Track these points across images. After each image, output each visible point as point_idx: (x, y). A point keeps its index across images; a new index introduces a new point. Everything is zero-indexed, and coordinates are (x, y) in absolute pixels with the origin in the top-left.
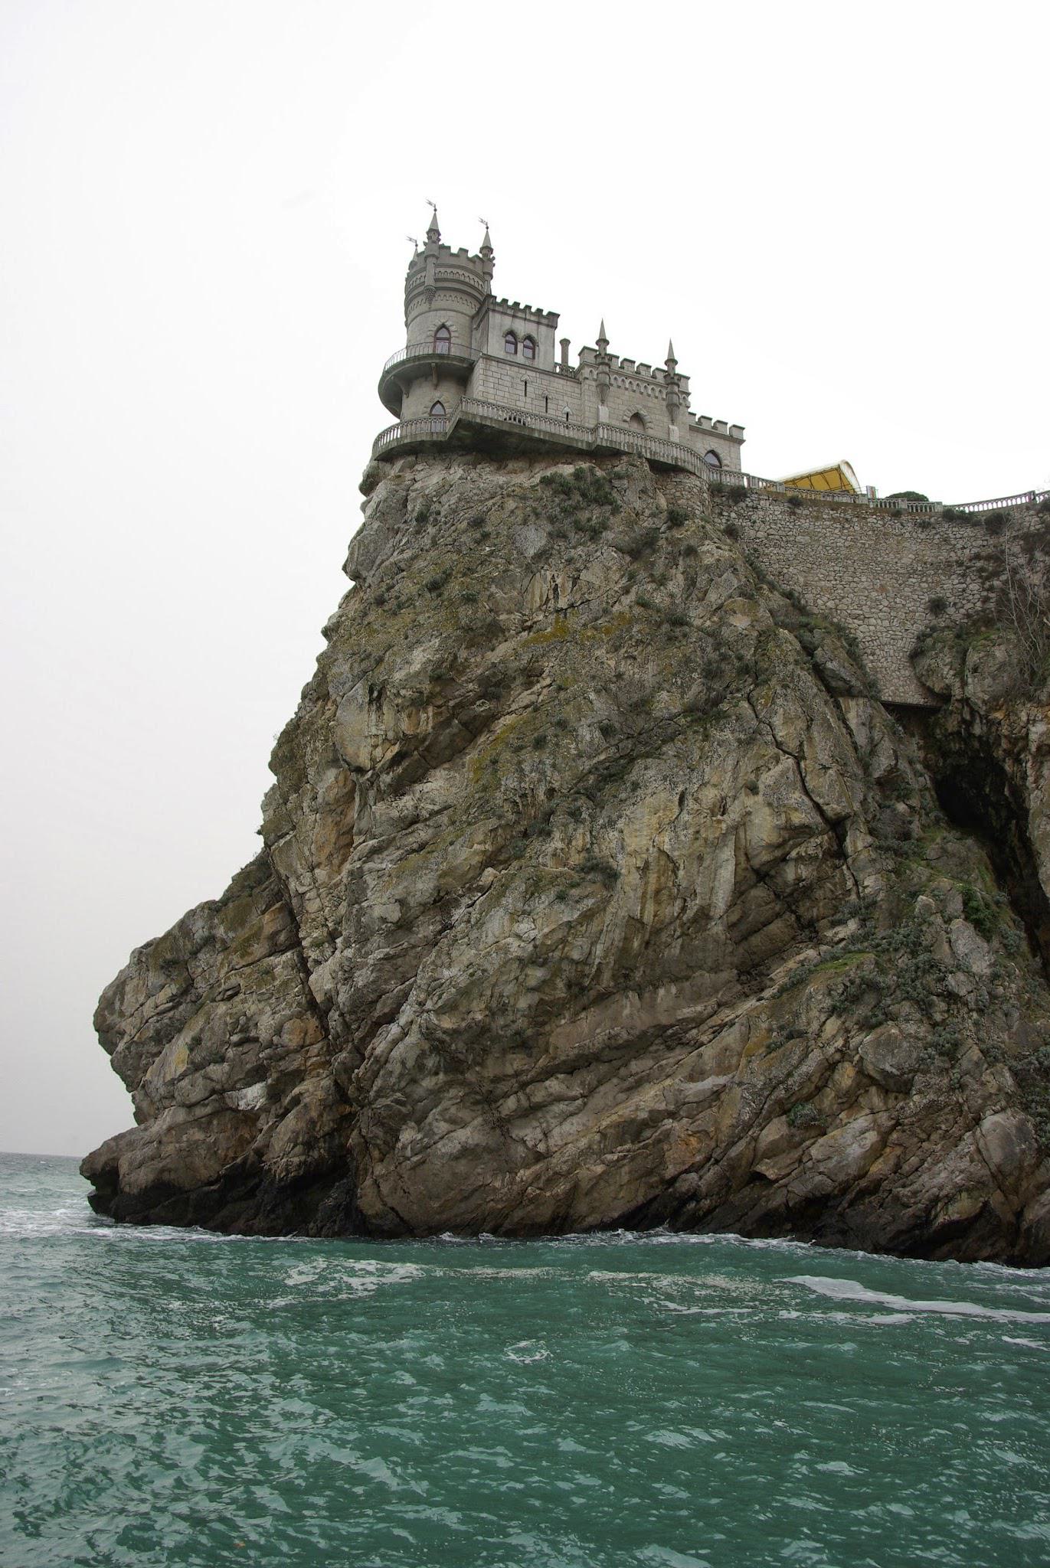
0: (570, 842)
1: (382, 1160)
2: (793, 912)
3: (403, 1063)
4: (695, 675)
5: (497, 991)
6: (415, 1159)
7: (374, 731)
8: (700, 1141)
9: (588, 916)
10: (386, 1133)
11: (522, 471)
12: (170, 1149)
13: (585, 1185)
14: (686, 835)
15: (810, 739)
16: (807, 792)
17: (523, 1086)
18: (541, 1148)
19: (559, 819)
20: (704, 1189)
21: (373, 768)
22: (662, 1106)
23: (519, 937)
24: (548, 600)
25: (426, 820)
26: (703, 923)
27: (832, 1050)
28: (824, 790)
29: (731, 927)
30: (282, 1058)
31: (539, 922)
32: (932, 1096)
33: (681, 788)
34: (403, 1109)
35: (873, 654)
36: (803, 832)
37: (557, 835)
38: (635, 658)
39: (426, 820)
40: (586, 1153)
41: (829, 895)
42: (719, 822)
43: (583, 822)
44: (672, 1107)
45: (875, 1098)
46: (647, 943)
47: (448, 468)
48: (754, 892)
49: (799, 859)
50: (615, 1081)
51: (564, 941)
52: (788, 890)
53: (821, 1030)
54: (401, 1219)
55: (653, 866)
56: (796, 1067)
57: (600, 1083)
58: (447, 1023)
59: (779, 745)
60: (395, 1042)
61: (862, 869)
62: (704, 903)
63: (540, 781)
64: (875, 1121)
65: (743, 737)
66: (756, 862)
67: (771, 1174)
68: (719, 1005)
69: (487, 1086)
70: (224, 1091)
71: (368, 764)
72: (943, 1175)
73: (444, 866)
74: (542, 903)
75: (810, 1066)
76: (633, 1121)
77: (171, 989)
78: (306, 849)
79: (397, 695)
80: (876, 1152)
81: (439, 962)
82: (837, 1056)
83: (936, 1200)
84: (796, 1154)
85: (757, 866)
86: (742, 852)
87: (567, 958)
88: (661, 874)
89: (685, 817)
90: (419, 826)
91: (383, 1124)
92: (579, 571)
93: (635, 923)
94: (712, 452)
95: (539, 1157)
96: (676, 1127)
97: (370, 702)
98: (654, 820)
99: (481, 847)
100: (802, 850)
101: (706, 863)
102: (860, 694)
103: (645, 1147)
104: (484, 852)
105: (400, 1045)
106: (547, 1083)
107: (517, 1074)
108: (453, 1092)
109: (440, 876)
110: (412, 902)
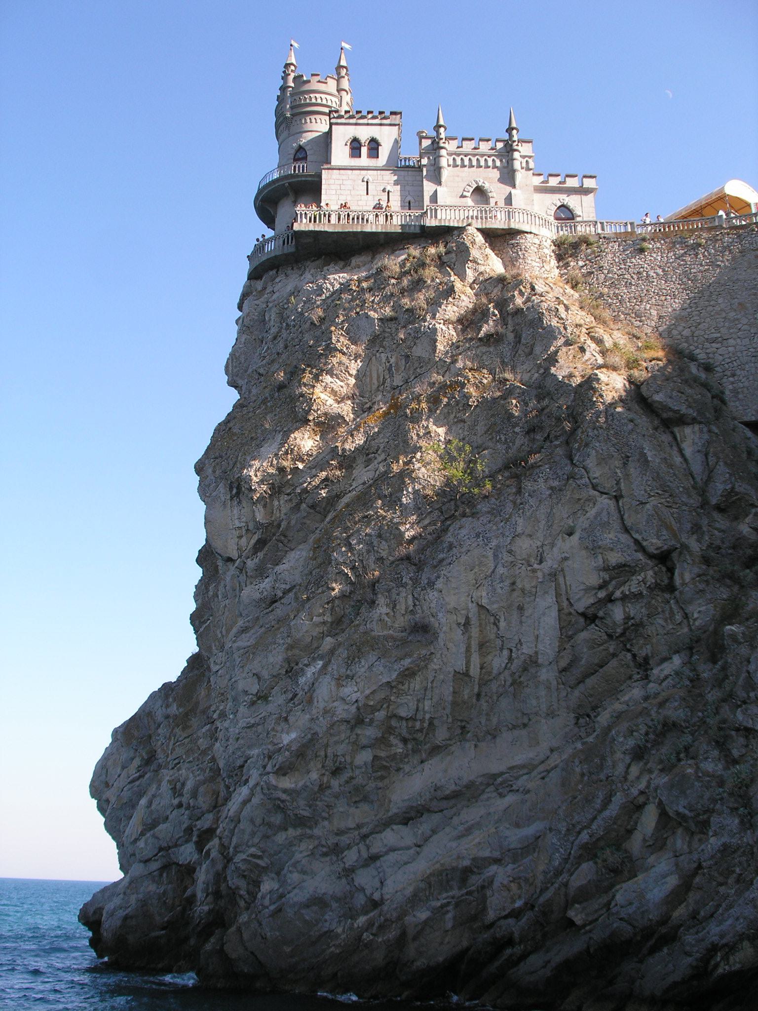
0: (394, 606)
1: (247, 909)
2: (629, 651)
3: (252, 821)
4: (517, 429)
5: (330, 751)
6: (272, 908)
7: (237, 524)
8: (520, 887)
9: (408, 674)
10: (248, 884)
11: (364, 265)
12: (133, 899)
13: (411, 932)
15: (627, 476)
16: (627, 530)
17: (364, 837)
18: (377, 896)
20: (516, 935)
21: (240, 557)
22: (486, 853)
25: (281, 598)
26: (533, 670)
27: (634, 792)
29: (564, 670)
30: (199, 819)
31: (361, 685)
32: (725, 839)
33: (494, 543)
34: (259, 862)
35: (733, 375)
36: (623, 570)
37: (381, 600)
38: (464, 421)
39: (281, 598)
40: (415, 900)
41: (661, 631)
42: (534, 571)
43: (404, 585)
44: (497, 854)
45: (679, 841)
46: (478, 695)
48: (584, 635)
49: (624, 598)
50: (447, 829)
51: (386, 700)
52: (619, 631)
53: (627, 772)
54: (260, 962)
55: (474, 621)
56: (600, 812)
57: (434, 832)
59: (594, 487)
61: (691, 601)
62: (531, 652)
63: (368, 552)
64: (677, 865)
65: (556, 483)
66: (581, 607)
67: (578, 920)
68: (552, 751)
69: (332, 840)
70: (170, 848)
71: (234, 554)
72: (729, 922)
73: (289, 640)
74: (361, 668)
75: (613, 810)
76: (454, 869)
77: (137, 762)
78: (218, 632)
80: (677, 896)
81: (279, 728)
82: (641, 799)
83: (714, 948)
84: (604, 899)
85: (581, 610)
86: (564, 598)
87: (395, 716)
89: (501, 570)
91: (244, 876)
92: (410, 348)
93: (463, 676)
95: (375, 904)
96: (501, 874)
97: (232, 498)
98: (471, 576)
99: (320, 619)
100: (625, 589)
101: (527, 614)
102: (694, 421)
103: (469, 893)
104: (324, 623)
105: (248, 805)
106: (383, 835)
107: (359, 827)
108: (303, 846)
109: (287, 649)
110: (265, 674)
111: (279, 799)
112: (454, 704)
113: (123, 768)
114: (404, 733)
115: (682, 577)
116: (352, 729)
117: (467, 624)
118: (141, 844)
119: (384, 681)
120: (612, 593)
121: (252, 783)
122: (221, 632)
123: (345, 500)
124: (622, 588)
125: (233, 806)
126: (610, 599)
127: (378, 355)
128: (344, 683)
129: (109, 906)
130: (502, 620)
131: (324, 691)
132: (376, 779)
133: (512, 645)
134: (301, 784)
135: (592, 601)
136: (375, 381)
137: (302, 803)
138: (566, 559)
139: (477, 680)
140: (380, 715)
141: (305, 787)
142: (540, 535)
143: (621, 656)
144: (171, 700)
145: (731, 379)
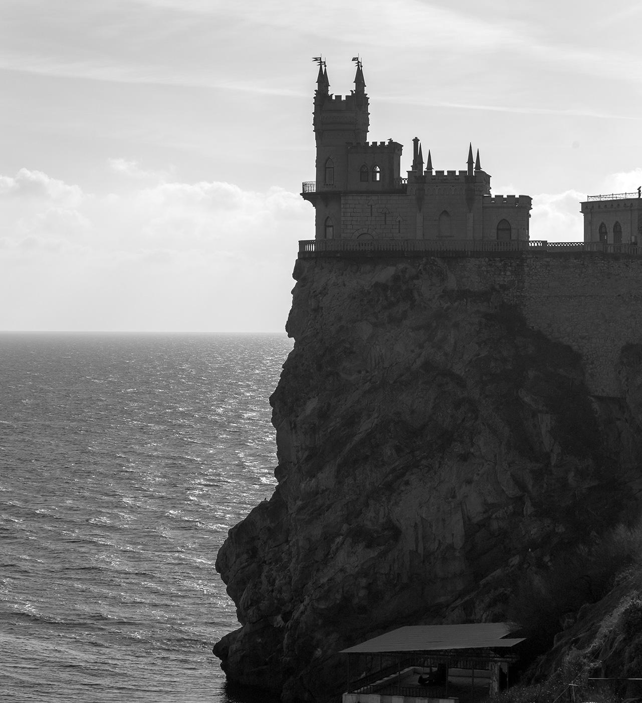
0: (379, 513)
19: (371, 502)
24: (379, 363)
35: (592, 363)
47: (330, 272)
49: (497, 518)
58: (322, 606)
60: (303, 613)
66: (475, 521)
74: (360, 548)
77: (245, 556)
79: (301, 428)
90: (319, 496)
94: (504, 219)
97: (291, 429)
113: (238, 556)
115: (527, 511)
118: (250, 612)
119: (371, 556)
121: (305, 603)
122: (293, 489)
123: (357, 439)
124: (496, 514)
125: (296, 615)
126: (489, 518)
127: (375, 346)
128: (351, 555)
129: (234, 647)
130: (434, 525)
131: (341, 558)
136: (373, 362)
138: (467, 496)
139: (422, 556)
144: (266, 516)
145: (591, 366)
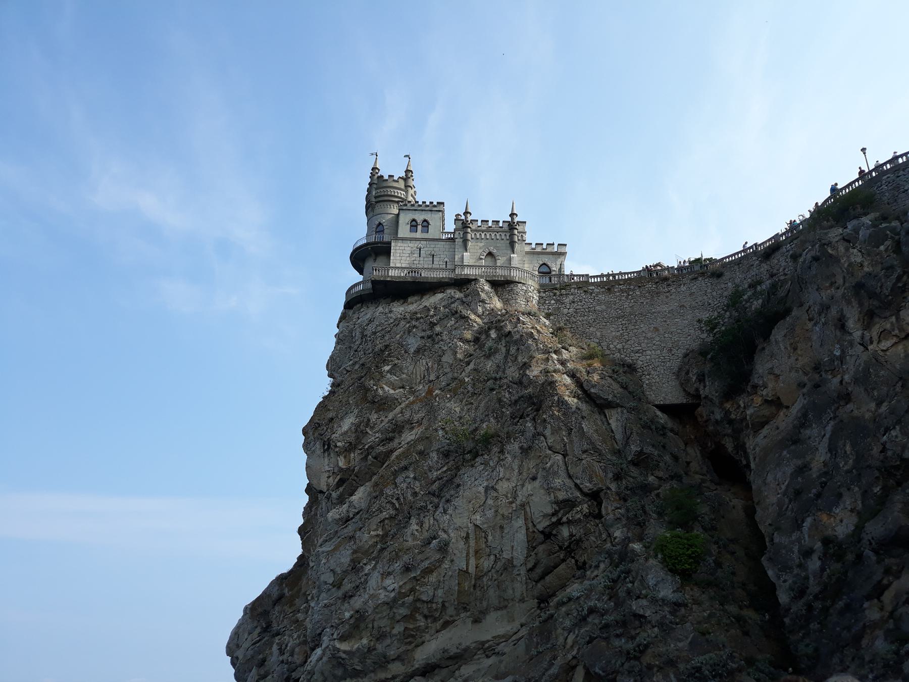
2: (573, 558)
3: (322, 673)
5: (376, 624)
14: (490, 514)
15: (571, 441)
16: (570, 477)
23: (385, 588)
24: (424, 376)
28: (579, 475)
29: (531, 570)
46: (474, 586)
49: (569, 522)
51: (412, 590)
52: (566, 544)
59: (550, 448)
62: (509, 557)
66: (540, 527)
85: (541, 529)
88: (477, 539)
89: (490, 502)
100: (569, 516)
111: (340, 657)
112: (459, 592)
114: (426, 612)
116: (391, 608)
117: (467, 538)
120: (561, 518)
121: (324, 646)
126: (559, 523)
132: (406, 644)
133: (496, 552)
134: (356, 646)
135: (548, 523)
137: (356, 660)
140: (411, 598)
141: (358, 649)
142: (514, 479)
143: (568, 561)
